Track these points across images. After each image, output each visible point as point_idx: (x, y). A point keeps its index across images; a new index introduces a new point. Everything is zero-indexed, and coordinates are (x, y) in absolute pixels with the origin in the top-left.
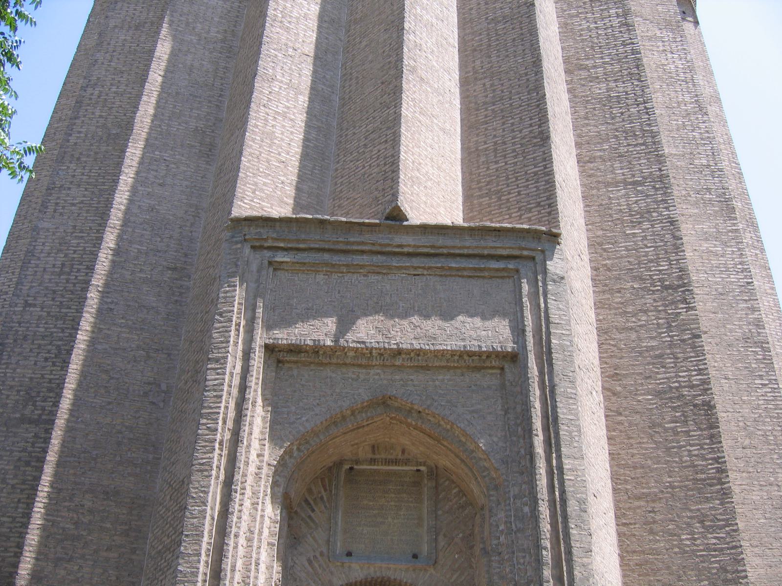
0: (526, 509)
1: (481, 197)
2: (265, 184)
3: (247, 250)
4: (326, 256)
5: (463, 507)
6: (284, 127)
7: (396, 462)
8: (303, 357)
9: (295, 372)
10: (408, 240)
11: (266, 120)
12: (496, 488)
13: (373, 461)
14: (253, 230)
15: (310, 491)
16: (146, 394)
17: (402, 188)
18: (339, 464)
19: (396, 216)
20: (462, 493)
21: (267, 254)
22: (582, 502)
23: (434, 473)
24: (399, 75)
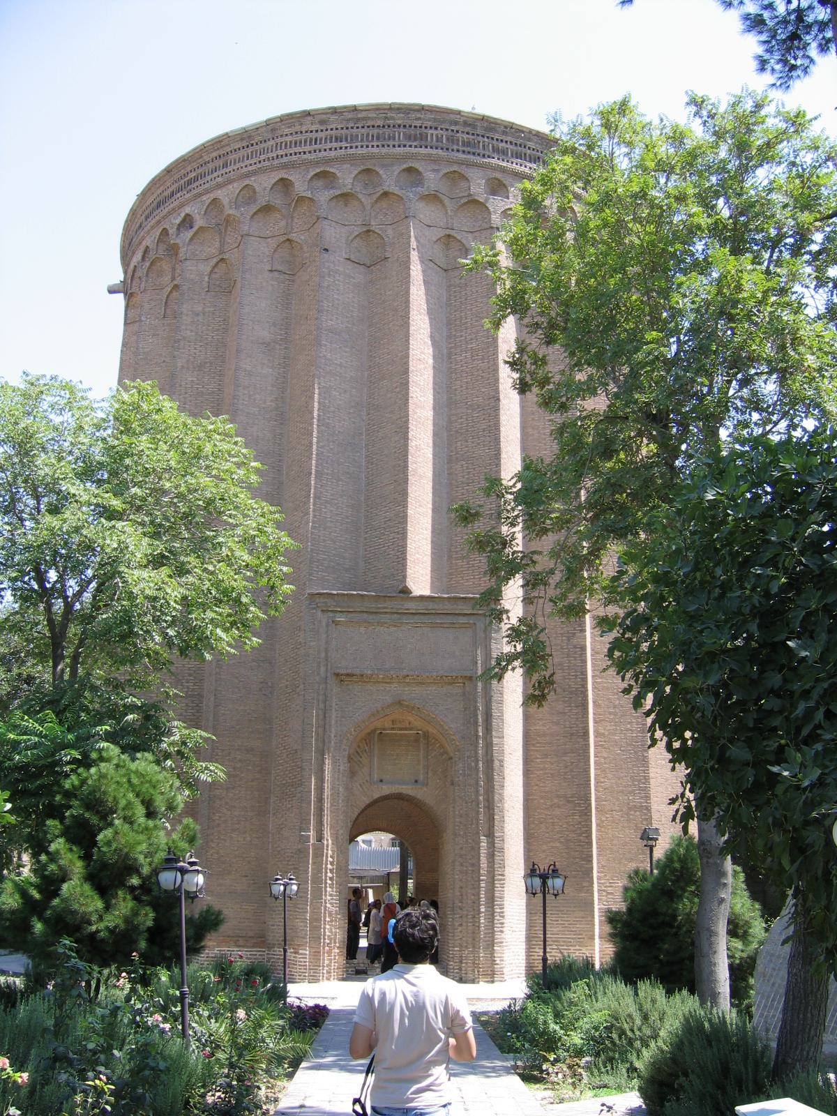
0: (473, 764)
1: (457, 559)
2: (324, 559)
3: (319, 613)
4: (365, 616)
5: (442, 755)
6: (331, 511)
7: (406, 729)
8: (354, 679)
9: (351, 687)
10: (412, 606)
11: (321, 509)
12: (459, 750)
13: (393, 729)
14: (322, 600)
15: (359, 746)
16: (260, 690)
17: (409, 571)
18: (374, 731)
19: (406, 591)
20: (442, 746)
21: (331, 615)
22: (501, 761)
23: (426, 735)
24: (406, 481)
